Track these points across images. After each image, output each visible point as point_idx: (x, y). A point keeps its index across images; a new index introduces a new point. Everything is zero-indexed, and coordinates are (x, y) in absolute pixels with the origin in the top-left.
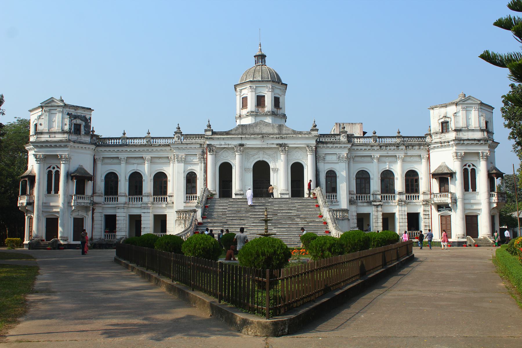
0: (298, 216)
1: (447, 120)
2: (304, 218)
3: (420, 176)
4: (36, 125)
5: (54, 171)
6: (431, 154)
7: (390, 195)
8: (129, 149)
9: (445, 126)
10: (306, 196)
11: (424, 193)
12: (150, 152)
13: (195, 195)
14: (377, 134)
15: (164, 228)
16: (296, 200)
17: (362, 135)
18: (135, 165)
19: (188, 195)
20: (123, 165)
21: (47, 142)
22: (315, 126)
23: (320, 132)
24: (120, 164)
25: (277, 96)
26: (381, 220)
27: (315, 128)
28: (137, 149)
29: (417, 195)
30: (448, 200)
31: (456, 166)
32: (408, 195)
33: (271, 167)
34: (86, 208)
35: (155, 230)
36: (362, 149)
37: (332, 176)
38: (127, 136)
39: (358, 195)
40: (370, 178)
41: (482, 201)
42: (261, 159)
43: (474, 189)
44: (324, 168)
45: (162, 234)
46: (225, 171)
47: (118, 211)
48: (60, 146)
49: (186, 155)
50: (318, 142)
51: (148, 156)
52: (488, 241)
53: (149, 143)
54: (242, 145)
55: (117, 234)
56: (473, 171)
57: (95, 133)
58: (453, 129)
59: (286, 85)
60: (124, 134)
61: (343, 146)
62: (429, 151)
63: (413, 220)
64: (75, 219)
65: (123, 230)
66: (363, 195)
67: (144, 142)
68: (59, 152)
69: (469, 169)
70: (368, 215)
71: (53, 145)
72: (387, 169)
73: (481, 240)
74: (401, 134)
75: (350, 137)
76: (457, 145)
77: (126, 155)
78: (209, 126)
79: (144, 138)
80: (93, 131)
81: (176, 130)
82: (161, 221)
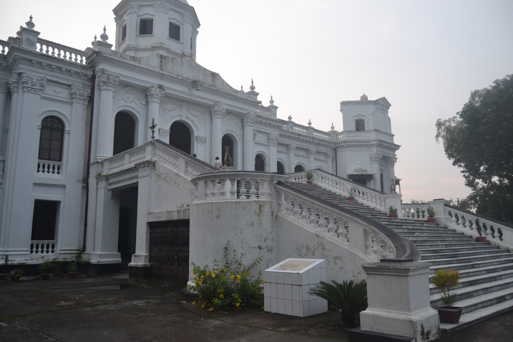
1: (363, 118)
6: (338, 154)
9: (360, 125)
13: (57, 163)
19: (42, 162)
22: (253, 88)
42: (184, 119)
54: (160, 87)
58: (372, 128)
59: (200, 25)
61: (277, 124)
62: (336, 150)
72: (301, 163)
74: (312, 125)
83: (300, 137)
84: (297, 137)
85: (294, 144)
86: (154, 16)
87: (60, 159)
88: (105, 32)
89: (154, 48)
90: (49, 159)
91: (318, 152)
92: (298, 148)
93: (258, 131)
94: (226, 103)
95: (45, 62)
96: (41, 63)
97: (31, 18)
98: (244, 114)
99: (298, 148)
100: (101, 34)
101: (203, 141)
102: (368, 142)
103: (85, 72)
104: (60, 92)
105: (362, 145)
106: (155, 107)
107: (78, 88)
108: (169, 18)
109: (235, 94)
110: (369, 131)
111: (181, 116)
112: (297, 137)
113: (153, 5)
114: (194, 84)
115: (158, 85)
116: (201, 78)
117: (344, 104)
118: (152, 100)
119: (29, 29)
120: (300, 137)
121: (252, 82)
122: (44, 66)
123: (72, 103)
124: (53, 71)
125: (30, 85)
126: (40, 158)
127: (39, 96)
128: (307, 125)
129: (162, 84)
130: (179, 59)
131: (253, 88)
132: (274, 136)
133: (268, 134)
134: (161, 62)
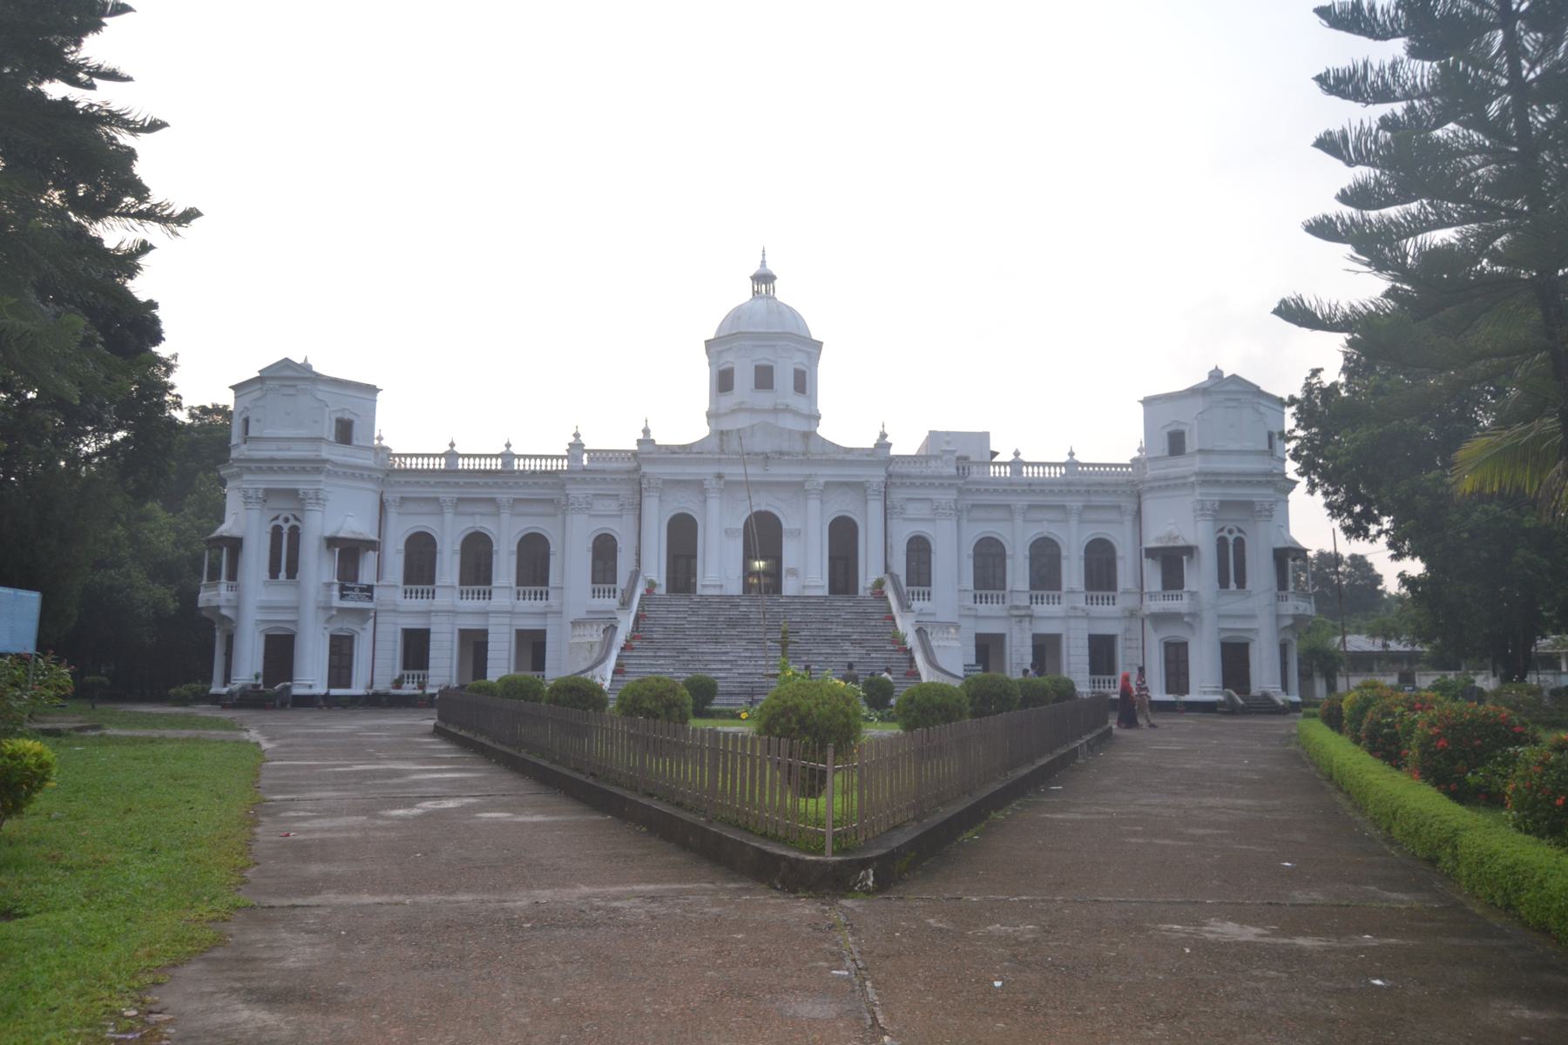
0: (846, 638)
1: (1181, 428)
2: (860, 643)
3: (1119, 553)
4: (247, 421)
5: (286, 528)
7: (1051, 593)
8: (462, 481)
9: (1176, 443)
10: (861, 592)
11: (1125, 592)
14: (1024, 457)
15: (539, 663)
16: (840, 601)
17: (987, 458)
18: (478, 518)
20: (449, 517)
21: (273, 460)
22: (883, 435)
23: (894, 451)
24: (442, 513)
26: (1030, 650)
27: (883, 444)
28: (481, 481)
29: (1111, 594)
30: (1180, 605)
31: (1199, 534)
32: (1090, 594)
33: (785, 526)
34: (362, 614)
35: (518, 667)
37: (919, 549)
38: (459, 449)
39: (978, 593)
40: (1002, 556)
41: (1261, 614)
42: (763, 508)
43: (1241, 583)
44: (902, 534)
45: (535, 674)
46: (683, 535)
47: (434, 619)
48: (304, 471)
50: (890, 476)
51: (503, 496)
52: (1273, 702)
54: (719, 476)
55: (431, 672)
56: (1240, 543)
57: (384, 443)
60: (452, 445)
62: (1139, 497)
63: (1102, 652)
64: (333, 638)
65: (443, 669)
66: (989, 592)
67: (497, 464)
68: (302, 483)
69: (1231, 539)
70: (1000, 639)
71: (286, 466)
73: (1256, 698)
75: (963, 462)
76: (1204, 483)
77: (454, 494)
78: (646, 431)
79: (497, 456)
80: (380, 438)
81: (572, 439)
82: (532, 645)
85: (1020, 502)
87: (615, 582)
89: (733, 411)
90: (605, 582)
91: (1087, 507)
94: (826, 474)
95: (588, 476)
101: (797, 533)
102: (1185, 477)
105: (1176, 485)
106: (714, 504)
109: (840, 457)
110: (1192, 455)
114: (766, 458)
116: (785, 447)
117: (1148, 402)
126: (594, 582)
128: (1065, 458)
131: (883, 435)
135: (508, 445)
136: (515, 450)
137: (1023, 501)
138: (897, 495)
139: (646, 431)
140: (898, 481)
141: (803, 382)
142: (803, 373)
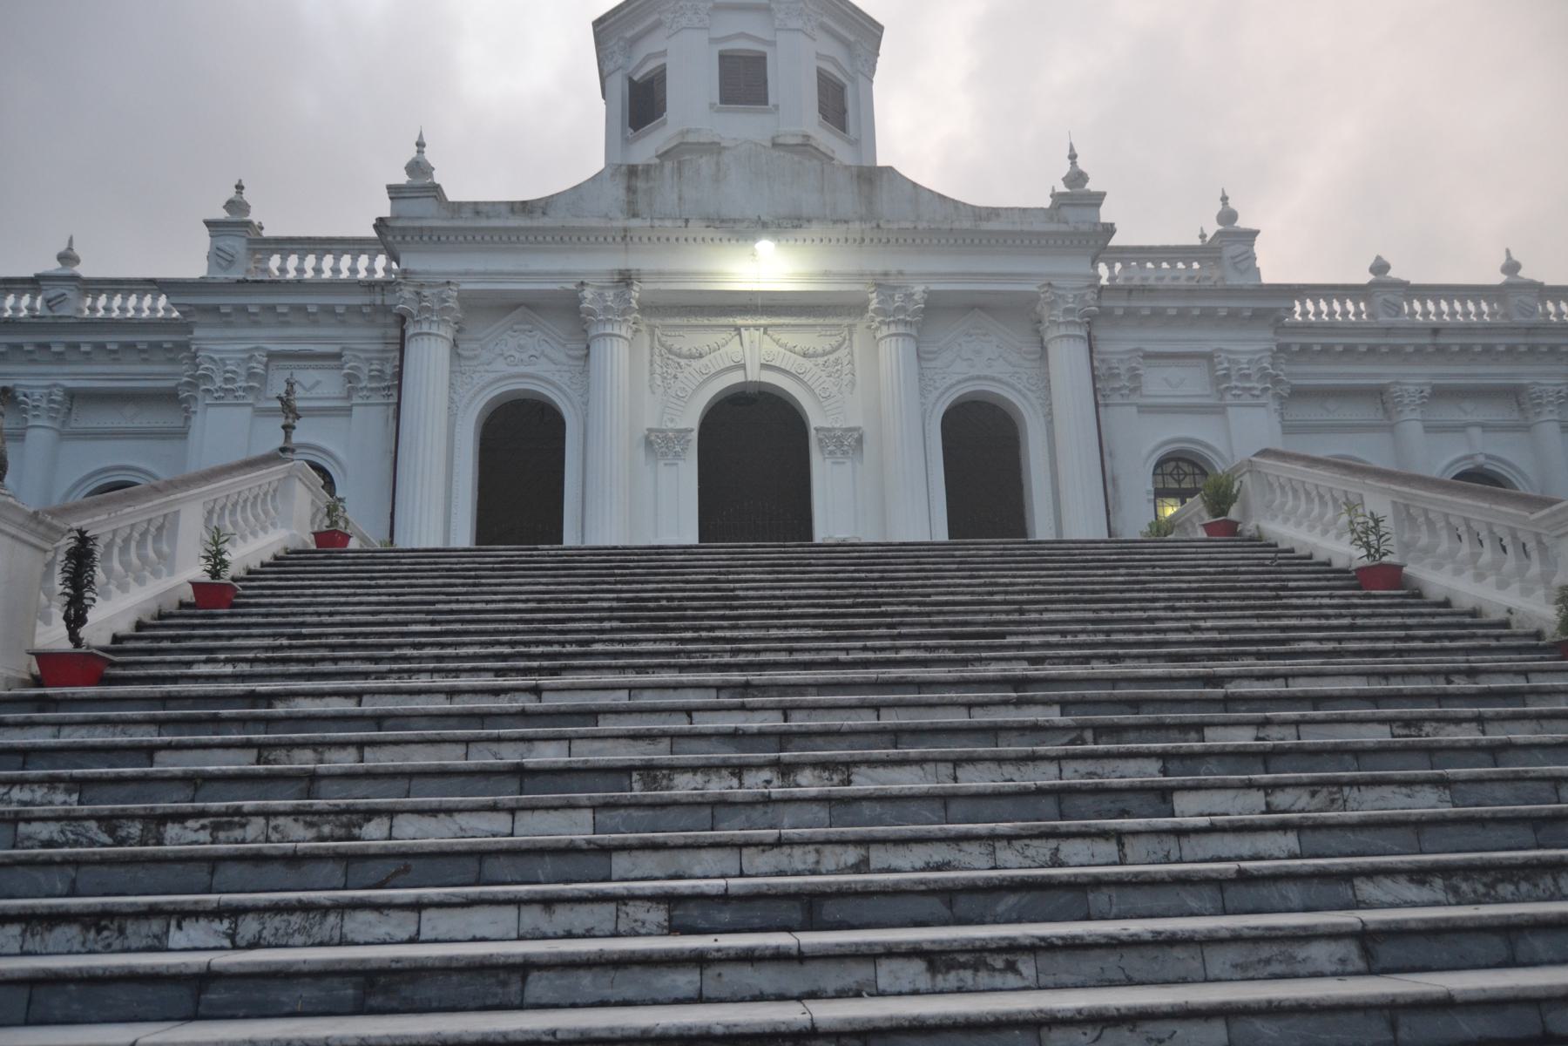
12: (59, 358)
22: (1076, 178)
25: (829, 68)
33: (816, 419)
36: (1326, 350)
42: (755, 375)
44: (1144, 440)
46: (523, 455)
49: (272, 356)
53: (66, 311)
54: (626, 279)
59: (880, 28)
72: (1481, 460)
74: (1525, 274)
78: (418, 167)
79: (34, 284)
81: (222, 215)
83: (1442, 340)
84: (1426, 340)
86: (664, 53)
88: (420, 152)
92: (1441, 394)
93: (1148, 356)
96: (243, 309)
97: (240, 187)
98: (1032, 299)
99: (1441, 394)
100: (409, 159)
101: (850, 443)
103: (379, 302)
104: (318, 383)
107: (362, 355)
108: (713, 41)
111: (743, 367)
112: (1426, 340)
113: (658, 25)
115: (611, 273)
118: (609, 330)
119: (236, 218)
120: (1442, 340)
121: (1073, 157)
122: (254, 314)
123: (350, 409)
124: (287, 324)
125: (219, 382)
127: (249, 410)
129: (622, 267)
130: (703, 160)
131: (1076, 178)
132: (1244, 359)
133: (1209, 357)
134: (631, 190)
135: (67, 258)
136: (85, 270)
137: (1415, 377)
138: (1120, 344)
139: (418, 167)
140: (1119, 304)
141: (841, 103)
142: (840, 90)
